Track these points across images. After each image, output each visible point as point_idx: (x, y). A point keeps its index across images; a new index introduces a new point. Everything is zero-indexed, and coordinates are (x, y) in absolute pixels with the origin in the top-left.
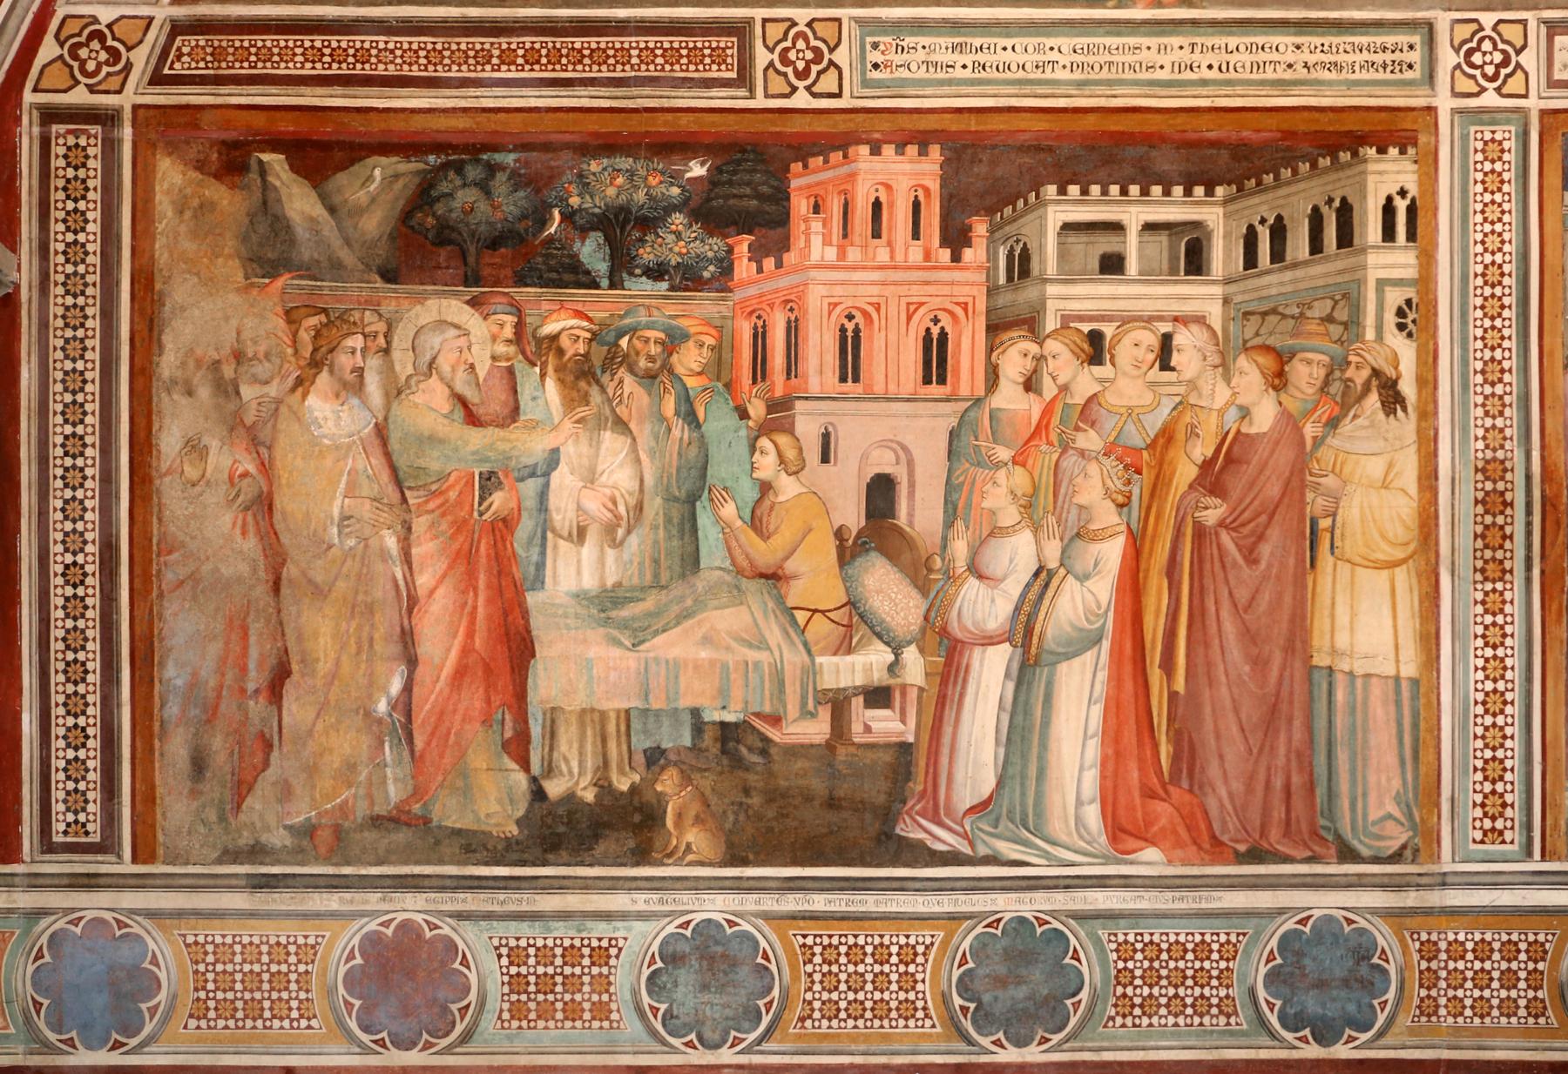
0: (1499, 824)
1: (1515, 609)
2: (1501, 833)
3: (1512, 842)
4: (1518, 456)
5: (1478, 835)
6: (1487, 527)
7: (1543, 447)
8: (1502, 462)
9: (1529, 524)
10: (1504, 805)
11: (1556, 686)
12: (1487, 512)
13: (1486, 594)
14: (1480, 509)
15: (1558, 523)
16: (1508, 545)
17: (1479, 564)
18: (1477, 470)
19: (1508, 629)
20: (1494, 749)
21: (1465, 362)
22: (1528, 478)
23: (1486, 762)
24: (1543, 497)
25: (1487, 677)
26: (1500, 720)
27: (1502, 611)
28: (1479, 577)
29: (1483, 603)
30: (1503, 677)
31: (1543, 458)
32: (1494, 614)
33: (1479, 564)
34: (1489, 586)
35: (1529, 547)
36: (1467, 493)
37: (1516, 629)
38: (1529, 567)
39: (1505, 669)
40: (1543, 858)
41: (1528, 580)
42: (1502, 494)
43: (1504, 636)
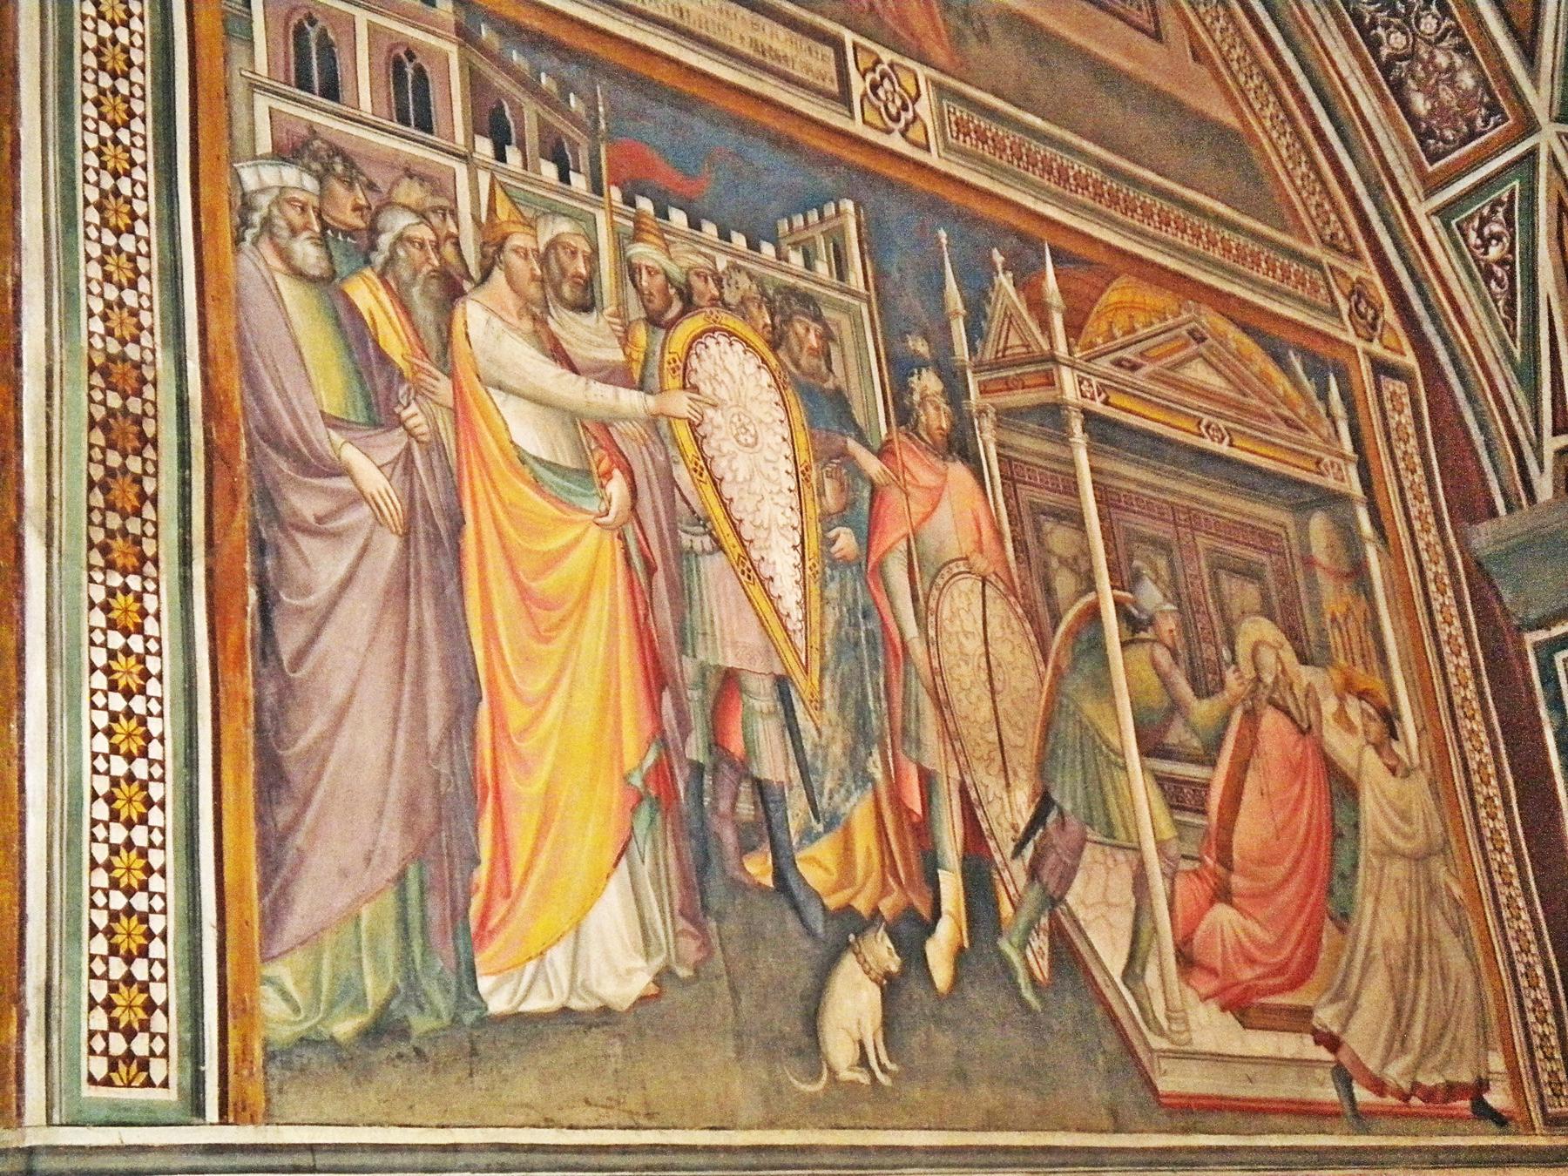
0: (140, 1046)
1: (163, 629)
2: (144, 1065)
3: (165, 1084)
4: (164, 364)
5: (100, 1068)
6: (110, 472)
7: (205, 360)
8: (138, 366)
9: (185, 484)
10: (150, 1007)
11: (238, 784)
12: (111, 445)
13: (111, 593)
14: (99, 438)
15: (234, 494)
16: (148, 511)
17: (99, 536)
18: (92, 368)
19: (153, 664)
20: (129, 892)
21: (68, 183)
22: (183, 404)
23: (114, 916)
24: (208, 442)
25: (115, 750)
26: (140, 836)
27: (140, 629)
28: (96, 558)
29: (106, 608)
30: (144, 753)
31: (206, 380)
32: (127, 633)
33: (99, 536)
34: (116, 580)
35: (185, 523)
36: (77, 401)
37: (165, 664)
38: (186, 560)
39: (148, 737)
40: (223, 1120)
41: (186, 583)
42: (138, 421)
43: (146, 675)
